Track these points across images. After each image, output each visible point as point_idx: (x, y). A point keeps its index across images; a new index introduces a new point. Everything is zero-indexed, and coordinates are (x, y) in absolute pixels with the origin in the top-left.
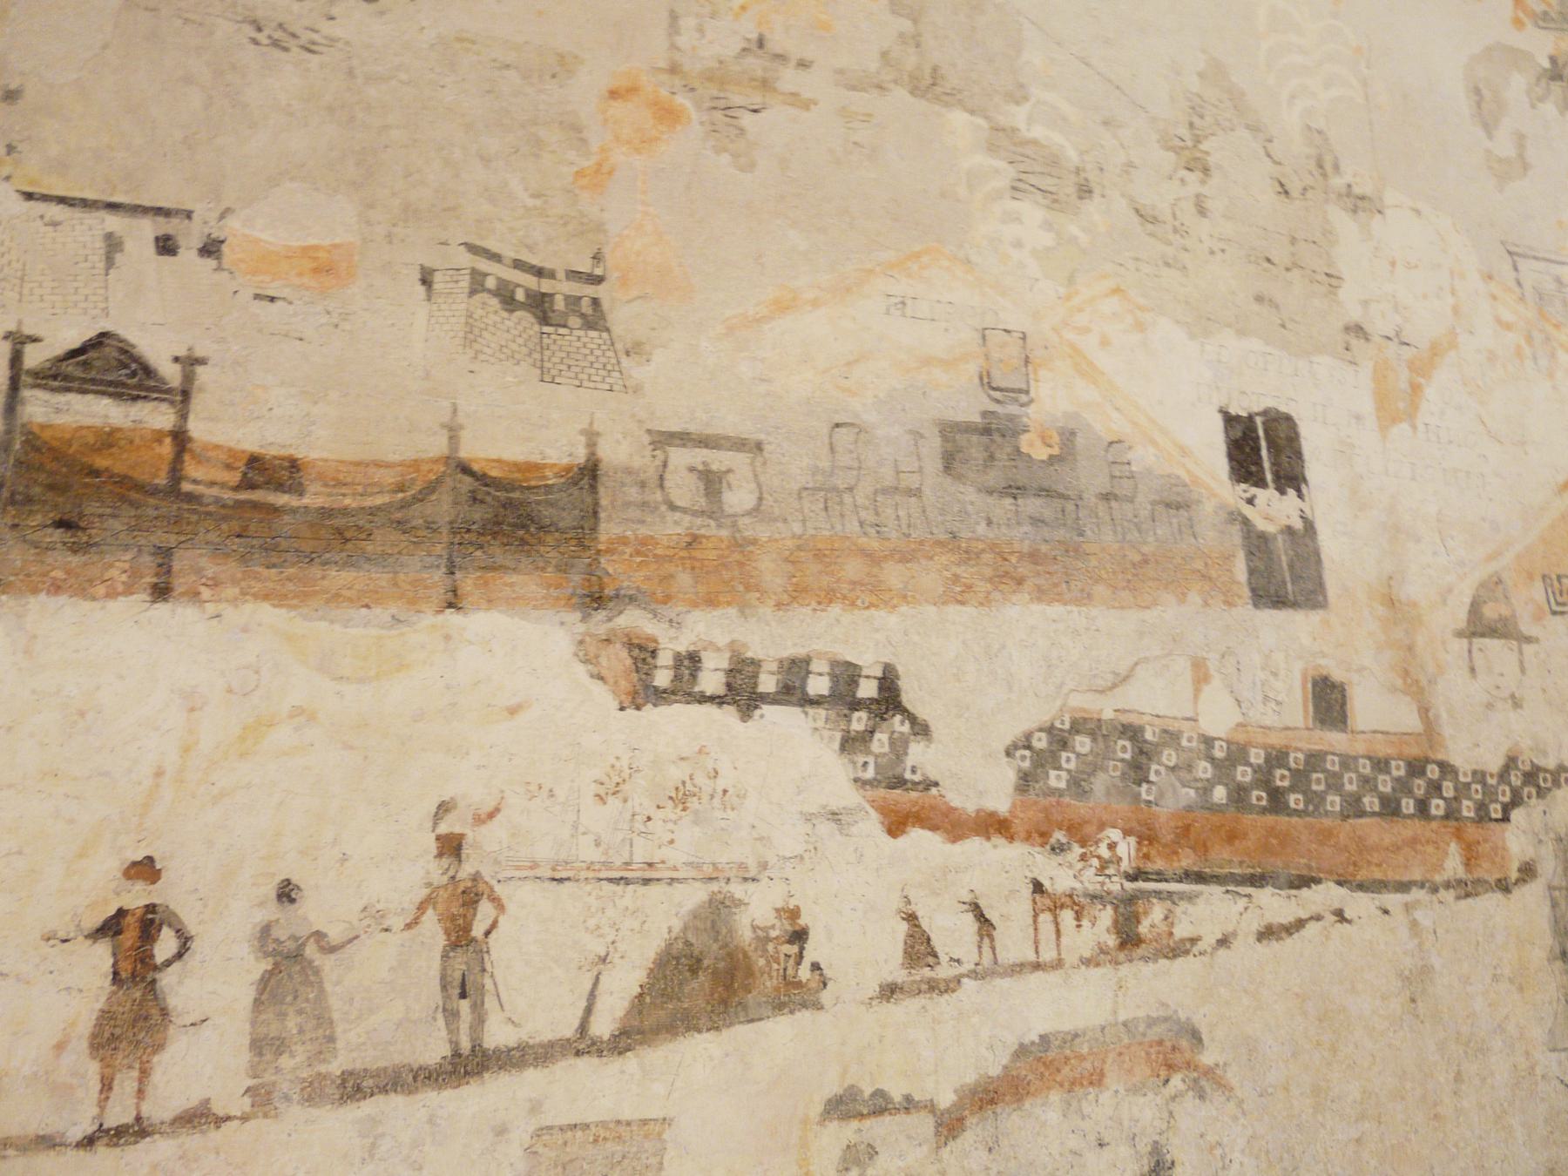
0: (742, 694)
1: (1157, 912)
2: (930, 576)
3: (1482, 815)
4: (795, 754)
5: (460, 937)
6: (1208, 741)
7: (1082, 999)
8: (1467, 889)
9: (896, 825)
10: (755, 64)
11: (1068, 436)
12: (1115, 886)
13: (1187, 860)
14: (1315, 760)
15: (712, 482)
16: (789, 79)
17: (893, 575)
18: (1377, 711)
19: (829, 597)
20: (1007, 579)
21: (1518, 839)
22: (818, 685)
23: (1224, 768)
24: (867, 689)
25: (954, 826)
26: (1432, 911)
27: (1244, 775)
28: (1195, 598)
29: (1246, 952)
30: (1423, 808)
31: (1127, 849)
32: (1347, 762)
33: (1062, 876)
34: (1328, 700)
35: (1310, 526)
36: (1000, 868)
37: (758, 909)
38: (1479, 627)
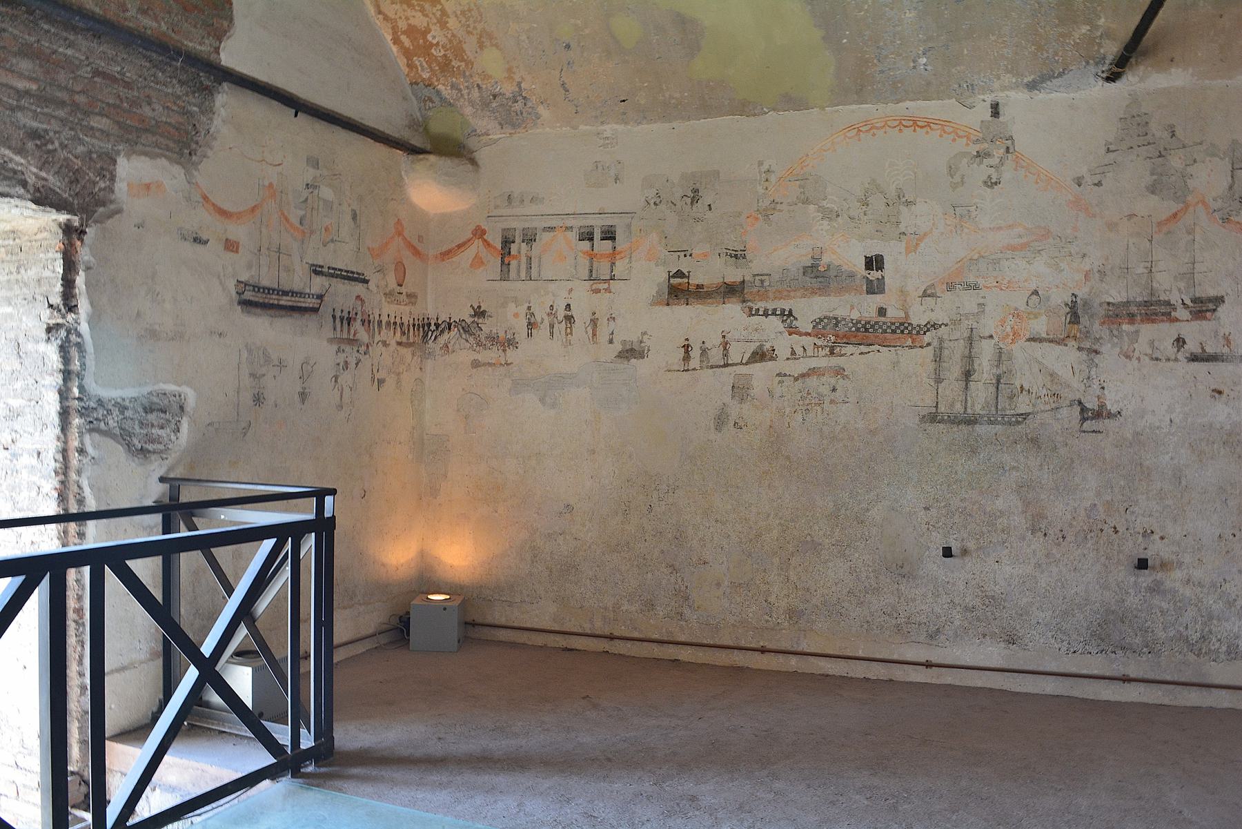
0: (766, 314)
2: (799, 294)
3: (918, 333)
4: (775, 323)
5: (725, 349)
7: (822, 362)
8: (911, 347)
14: (877, 323)
15: (762, 281)
16: (779, 206)
17: (792, 294)
18: (893, 313)
21: (927, 338)
25: (801, 334)
26: (900, 351)
29: (856, 357)
30: (902, 332)
33: (819, 342)
34: (882, 312)
36: (808, 341)
37: (767, 346)
38: (925, 295)
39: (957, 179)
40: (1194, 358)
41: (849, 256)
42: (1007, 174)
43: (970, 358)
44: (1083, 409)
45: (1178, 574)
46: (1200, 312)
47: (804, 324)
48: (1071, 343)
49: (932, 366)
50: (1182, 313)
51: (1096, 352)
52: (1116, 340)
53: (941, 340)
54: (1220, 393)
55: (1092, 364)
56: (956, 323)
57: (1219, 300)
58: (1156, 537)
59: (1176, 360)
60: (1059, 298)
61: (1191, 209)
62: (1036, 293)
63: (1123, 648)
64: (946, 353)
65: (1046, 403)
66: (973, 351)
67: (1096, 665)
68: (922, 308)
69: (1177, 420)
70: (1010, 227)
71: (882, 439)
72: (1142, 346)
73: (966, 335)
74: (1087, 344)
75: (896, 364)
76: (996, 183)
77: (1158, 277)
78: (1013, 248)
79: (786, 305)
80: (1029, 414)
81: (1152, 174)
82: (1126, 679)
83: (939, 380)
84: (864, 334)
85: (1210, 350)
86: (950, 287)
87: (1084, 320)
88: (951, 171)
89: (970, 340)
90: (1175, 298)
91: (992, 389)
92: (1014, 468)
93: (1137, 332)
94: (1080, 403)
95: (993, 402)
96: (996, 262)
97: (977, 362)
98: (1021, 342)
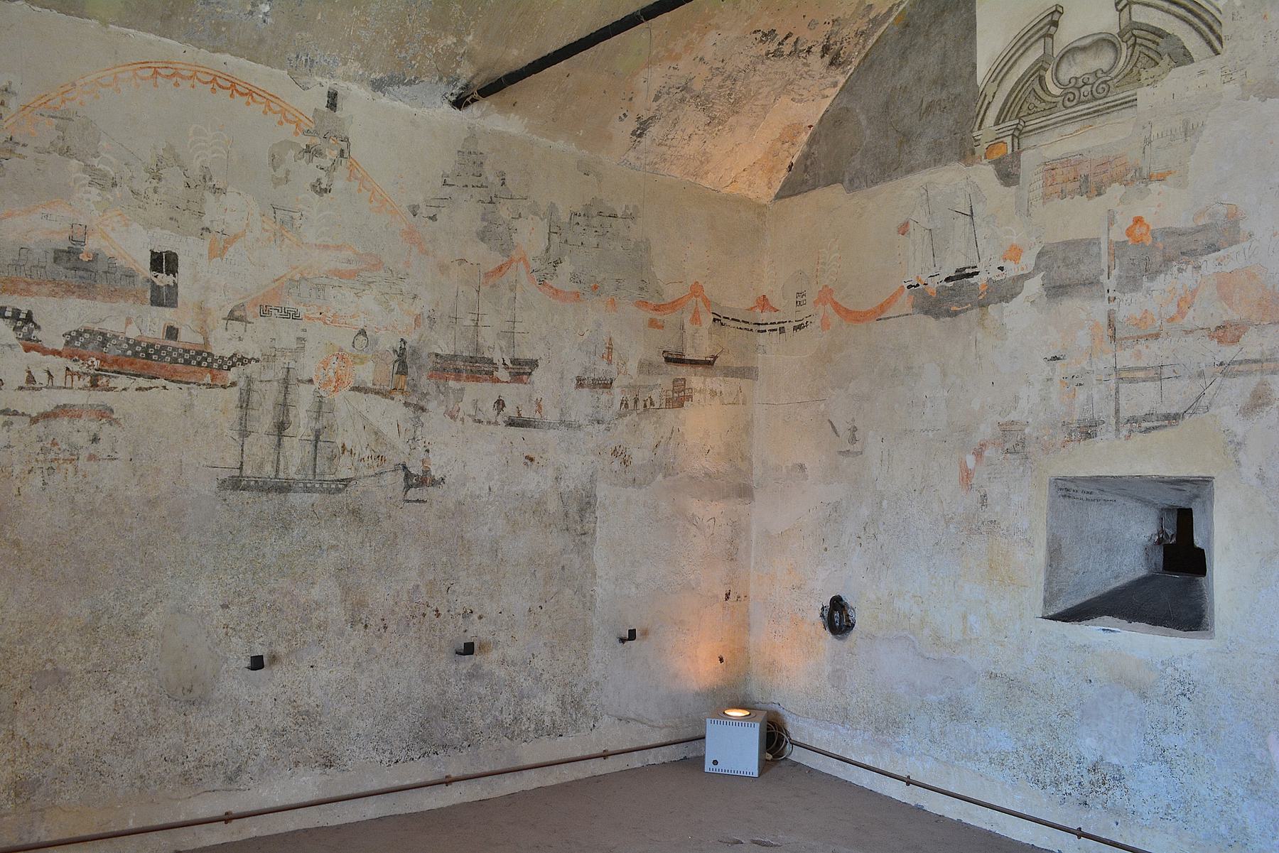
1: (105, 379)
2: (45, 290)
6: (128, 339)
8: (210, 386)
9: (27, 350)
10: (9, 145)
11: (96, 255)
12: (92, 372)
13: (116, 368)
14: (164, 347)
16: (19, 149)
17: (34, 288)
18: (188, 337)
19: (14, 292)
20: (69, 291)
21: (232, 375)
22: (8, 314)
23: (131, 347)
24: (22, 316)
25: (45, 352)
26: (195, 390)
27: (138, 349)
28: (131, 301)
30: (199, 364)
31: (97, 363)
32: (174, 349)
33: (75, 367)
34: (172, 332)
35: (176, 285)
39: (280, 173)
40: (511, 423)
41: (131, 246)
42: (338, 185)
43: (284, 406)
44: (408, 475)
45: (494, 655)
46: (518, 374)
47: (52, 336)
48: (398, 396)
49: (235, 414)
50: (502, 374)
51: (423, 409)
52: (442, 397)
53: (250, 381)
54: (532, 460)
55: (418, 423)
56: (270, 358)
57: (534, 364)
58: (475, 616)
59: (496, 423)
60: (388, 342)
61: (514, 264)
62: (363, 332)
63: (444, 746)
64: (255, 397)
65: (369, 467)
66: (289, 397)
67: (419, 771)
68: (227, 335)
69: (495, 489)
70: (338, 248)
71: (165, 513)
72: (466, 407)
73: (281, 375)
74: (414, 400)
75: (188, 408)
76: (326, 190)
77: (483, 331)
78: (340, 274)
79: (23, 304)
80: (351, 479)
81: (483, 219)
82: (448, 781)
83: (244, 433)
84: (145, 361)
85: (525, 415)
86: (265, 312)
87: (412, 371)
88: (275, 161)
89: (286, 383)
90: (497, 357)
91: (309, 448)
92: (333, 547)
93: (462, 389)
94: (405, 467)
95: (310, 464)
96: (320, 288)
97: (292, 412)
98: (344, 391)
